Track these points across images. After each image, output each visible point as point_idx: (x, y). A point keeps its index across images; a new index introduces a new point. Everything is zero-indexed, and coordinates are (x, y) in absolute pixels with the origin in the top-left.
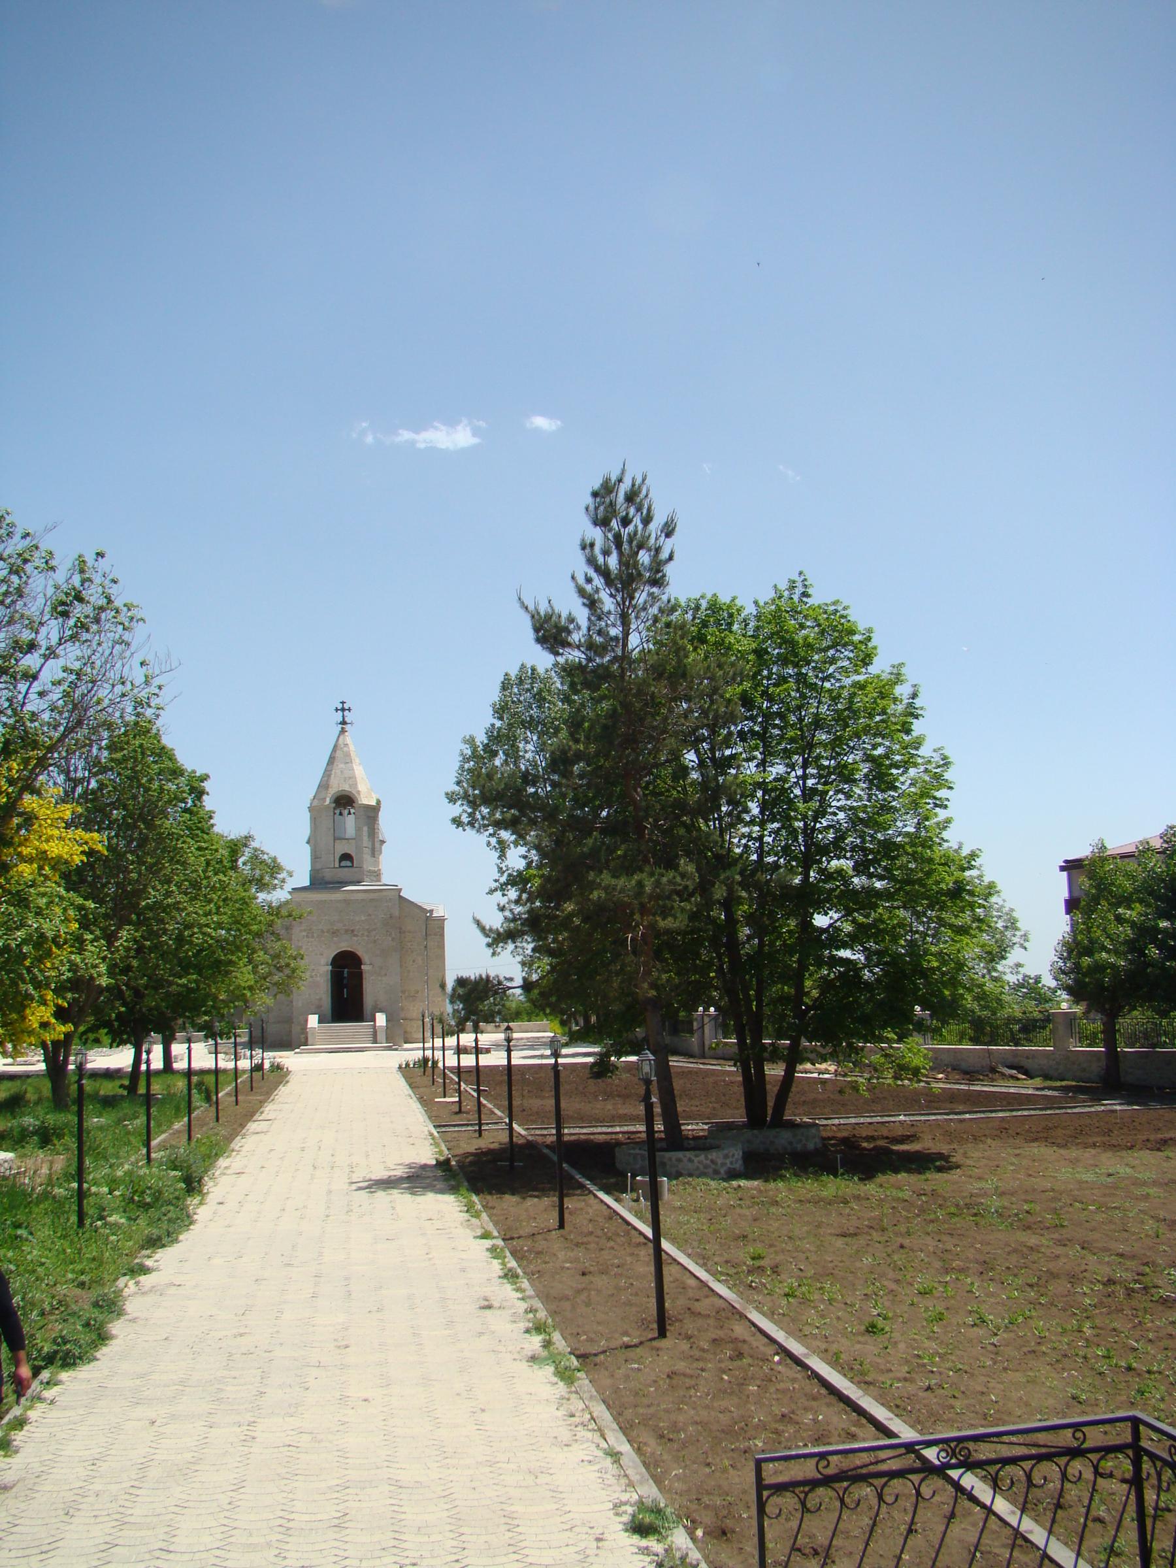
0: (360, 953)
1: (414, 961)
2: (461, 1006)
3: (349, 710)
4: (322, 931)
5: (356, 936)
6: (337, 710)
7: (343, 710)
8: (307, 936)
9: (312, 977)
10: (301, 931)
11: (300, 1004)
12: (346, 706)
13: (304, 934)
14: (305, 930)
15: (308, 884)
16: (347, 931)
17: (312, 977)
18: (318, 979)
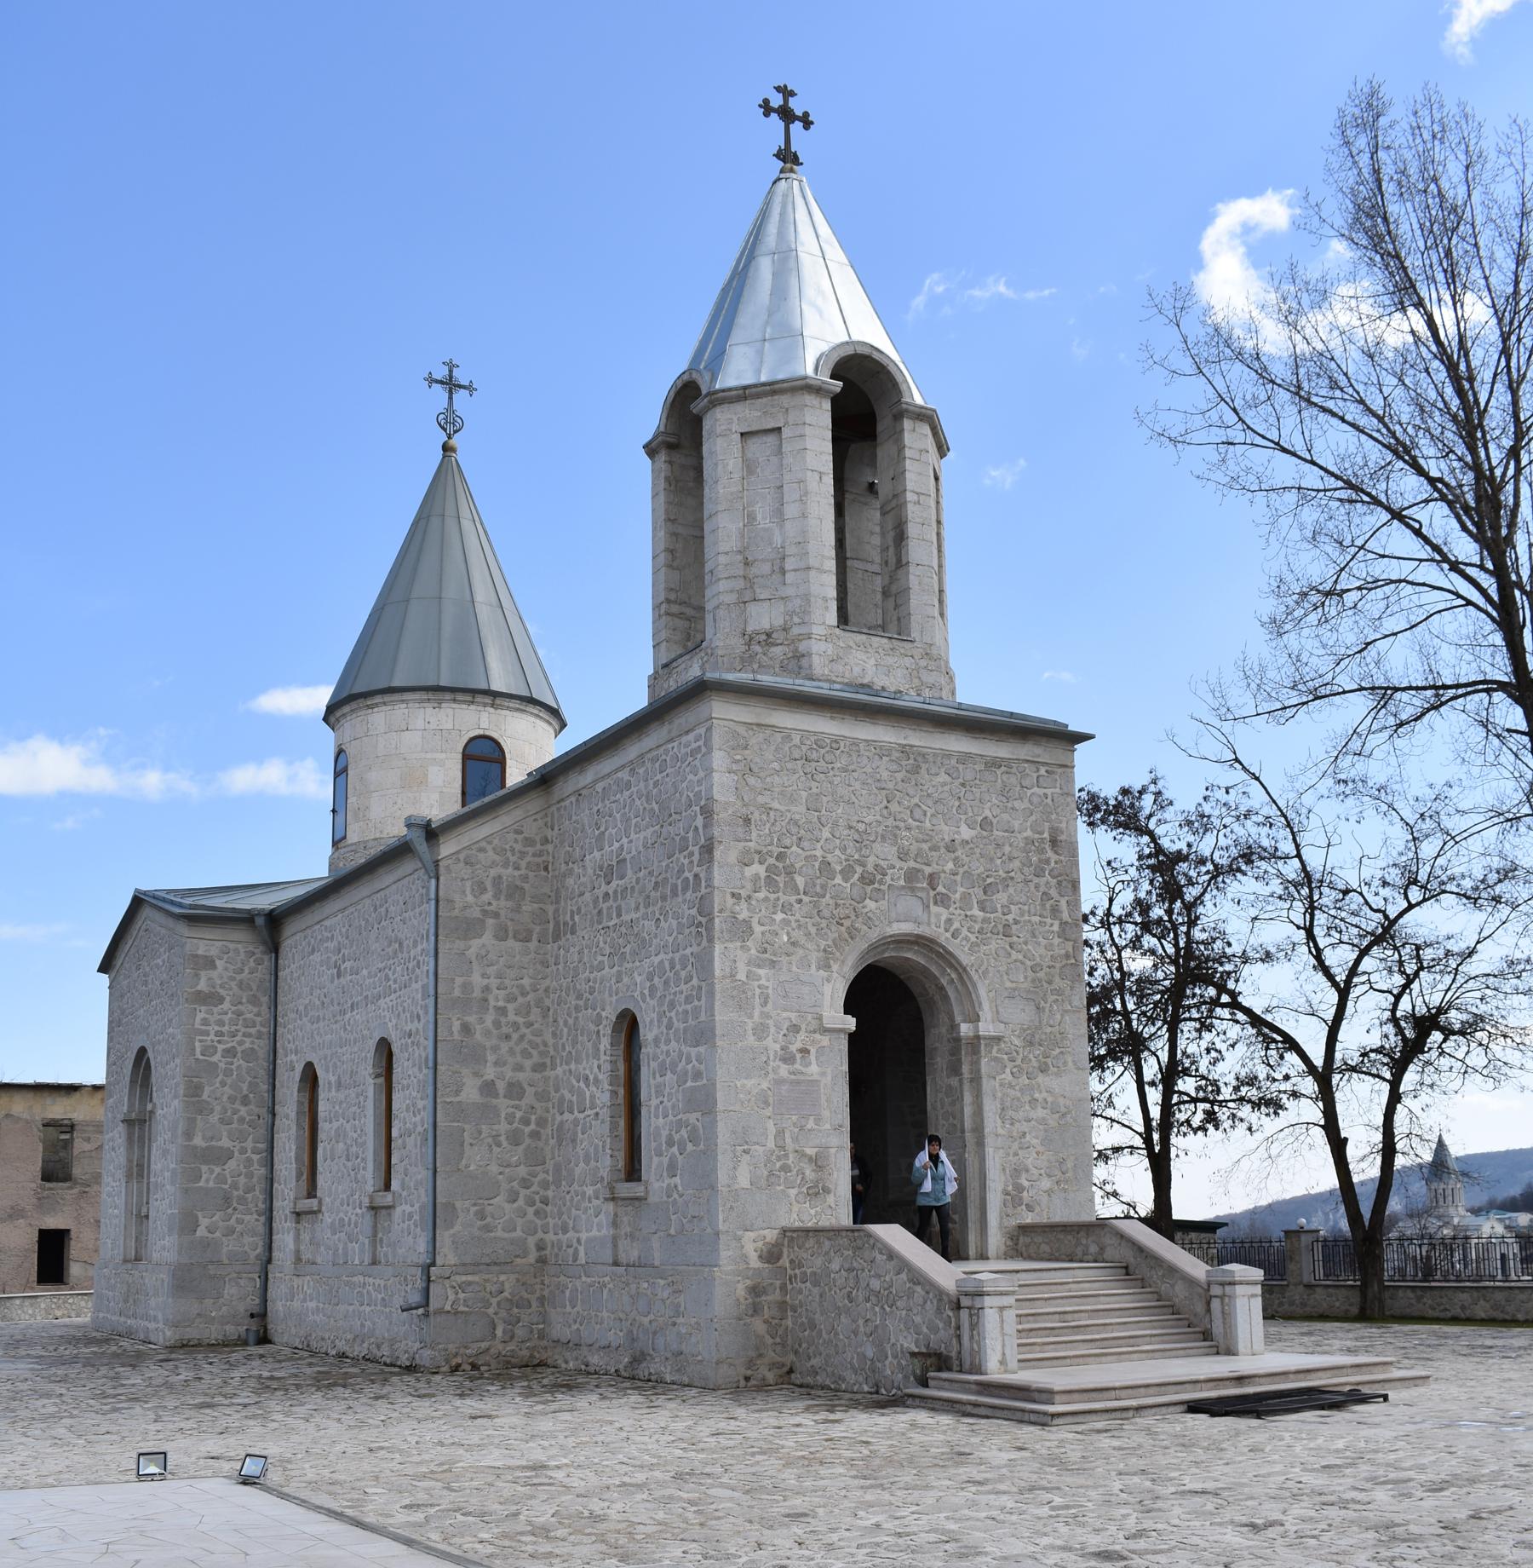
5: (942, 900)
9: (788, 1059)
11: (743, 1181)
13: (758, 869)
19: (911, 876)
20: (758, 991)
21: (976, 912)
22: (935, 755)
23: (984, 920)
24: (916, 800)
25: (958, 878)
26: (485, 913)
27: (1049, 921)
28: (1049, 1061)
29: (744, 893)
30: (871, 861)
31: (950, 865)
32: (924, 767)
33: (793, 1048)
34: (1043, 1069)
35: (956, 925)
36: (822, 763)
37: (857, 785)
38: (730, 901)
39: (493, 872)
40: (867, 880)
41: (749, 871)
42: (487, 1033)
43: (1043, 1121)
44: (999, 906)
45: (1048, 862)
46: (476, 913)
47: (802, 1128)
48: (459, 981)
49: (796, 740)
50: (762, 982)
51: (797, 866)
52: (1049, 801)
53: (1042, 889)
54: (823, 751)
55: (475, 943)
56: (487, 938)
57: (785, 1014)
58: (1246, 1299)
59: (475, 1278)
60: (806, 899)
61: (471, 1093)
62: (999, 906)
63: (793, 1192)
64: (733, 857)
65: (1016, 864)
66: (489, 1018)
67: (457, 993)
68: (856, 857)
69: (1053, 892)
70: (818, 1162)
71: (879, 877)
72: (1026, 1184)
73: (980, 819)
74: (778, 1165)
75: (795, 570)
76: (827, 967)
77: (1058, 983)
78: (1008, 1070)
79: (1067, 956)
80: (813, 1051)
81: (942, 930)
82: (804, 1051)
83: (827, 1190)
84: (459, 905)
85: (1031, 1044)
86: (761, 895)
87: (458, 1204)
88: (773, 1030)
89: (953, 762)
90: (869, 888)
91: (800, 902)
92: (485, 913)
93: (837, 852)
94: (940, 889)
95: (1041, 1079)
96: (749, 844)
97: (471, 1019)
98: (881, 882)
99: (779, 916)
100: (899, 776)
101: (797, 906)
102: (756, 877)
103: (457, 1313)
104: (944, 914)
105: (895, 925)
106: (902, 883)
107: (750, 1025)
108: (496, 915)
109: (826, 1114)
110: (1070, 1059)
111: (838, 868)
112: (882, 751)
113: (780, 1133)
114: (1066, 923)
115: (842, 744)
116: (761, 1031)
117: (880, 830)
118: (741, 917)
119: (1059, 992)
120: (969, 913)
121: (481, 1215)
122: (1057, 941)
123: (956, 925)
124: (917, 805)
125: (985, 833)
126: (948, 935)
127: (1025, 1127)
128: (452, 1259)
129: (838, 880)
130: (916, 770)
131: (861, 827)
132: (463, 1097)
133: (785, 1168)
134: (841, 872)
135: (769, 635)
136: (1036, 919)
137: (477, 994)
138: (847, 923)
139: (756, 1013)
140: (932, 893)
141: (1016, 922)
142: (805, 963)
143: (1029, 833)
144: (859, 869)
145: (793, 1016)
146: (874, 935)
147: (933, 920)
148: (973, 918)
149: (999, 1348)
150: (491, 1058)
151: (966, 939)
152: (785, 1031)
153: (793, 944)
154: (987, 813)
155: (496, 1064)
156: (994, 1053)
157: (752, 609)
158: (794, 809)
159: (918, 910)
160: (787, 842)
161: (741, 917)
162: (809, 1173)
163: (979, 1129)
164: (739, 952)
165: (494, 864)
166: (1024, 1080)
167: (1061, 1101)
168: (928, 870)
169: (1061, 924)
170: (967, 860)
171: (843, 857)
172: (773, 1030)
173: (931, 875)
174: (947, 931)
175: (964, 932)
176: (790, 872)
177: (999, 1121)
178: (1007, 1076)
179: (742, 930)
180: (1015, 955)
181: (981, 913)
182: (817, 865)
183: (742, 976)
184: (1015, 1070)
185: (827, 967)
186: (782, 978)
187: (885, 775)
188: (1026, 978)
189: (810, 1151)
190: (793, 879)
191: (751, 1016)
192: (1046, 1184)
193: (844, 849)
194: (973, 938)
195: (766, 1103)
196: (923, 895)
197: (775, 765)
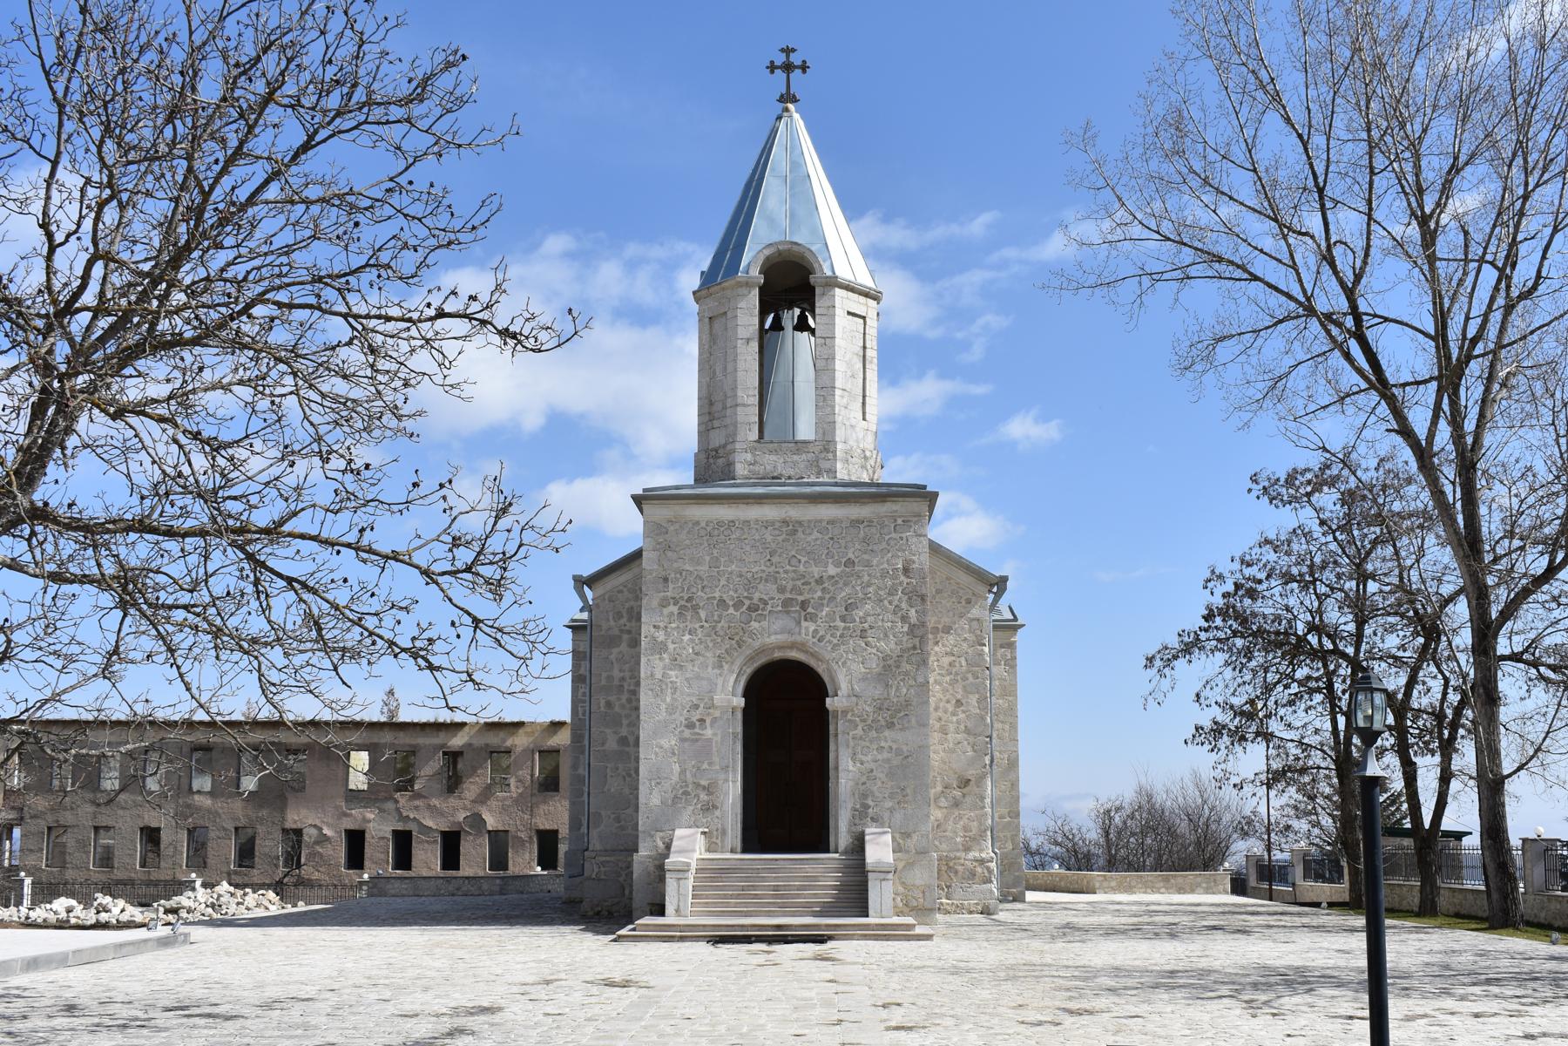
1: (959, 703)
2: (1392, 740)
3: (804, 67)
4: (722, 602)
5: (811, 618)
6: (772, 67)
7: (788, 68)
9: (691, 726)
11: (655, 800)
12: (796, 59)
13: (674, 609)
15: (688, 477)
17: (691, 726)
18: (709, 732)
19: (787, 603)
22: (809, 521)
23: (845, 628)
25: (825, 602)
26: (621, 631)
28: (895, 720)
29: (662, 624)
30: (757, 596)
31: (819, 594)
32: (800, 529)
34: (890, 725)
36: (722, 537)
37: (748, 548)
38: (652, 630)
39: (627, 605)
41: (666, 611)
42: (623, 706)
43: (888, 761)
45: (901, 583)
46: (616, 632)
47: (699, 769)
48: (604, 675)
49: (703, 524)
50: (674, 679)
53: (896, 603)
55: (615, 651)
56: (624, 647)
59: (612, 859)
60: (706, 625)
61: (612, 744)
64: (655, 603)
66: (624, 698)
67: (603, 682)
69: (904, 605)
72: (871, 803)
73: (844, 560)
76: (721, 667)
77: (906, 667)
78: (860, 728)
79: (914, 648)
82: (702, 721)
83: (715, 807)
84: (604, 626)
85: (880, 709)
86: (673, 625)
87: (603, 813)
89: (824, 524)
90: (754, 615)
91: (702, 627)
92: (621, 631)
93: (731, 593)
94: (810, 610)
95: (887, 733)
97: (612, 698)
98: (763, 609)
99: (687, 637)
100: (780, 538)
101: (700, 630)
102: (672, 613)
103: (599, 880)
104: (812, 627)
105: (773, 637)
107: (663, 706)
108: (629, 632)
109: (716, 759)
110: (913, 720)
111: (731, 603)
112: (767, 524)
113: (683, 772)
117: (764, 575)
118: (659, 640)
119: (907, 673)
121: (618, 820)
127: (872, 765)
128: (598, 847)
129: (731, 610)
131: (749, 575)
132: (607, 747)
133: (686, 793)
134: (734, 605)
137: (616, 682)
138: (737, 638)
139: (668, 700)
140: (803, 614)
141: (871, 627)
142: (704, 666)
144: (747, 602)
146: (757, 644)
147: (803, 631)
148: (836, 628)
150: (625, 722)
151: (830, 642)
153: (696, 654)
154: (851, 555)
155: (629, 725)
156: (849, 717)
157: (712, 432)
158: (699, 568)
159: (792, 624)
160: (694, 590)
161: (659, 640)
162: (703, 796)
163: (837, 768)
164: (657, 662)
165: (628, 600)
166: (873, 734)
167: (905, 748)
168: (800, 598)
170: (832, 589)
175: (828, 637)
176: (695, 608)
177: (851, 763)
178: (859, 731)
179: (660, 648)
183: (658, 676)
186: (688, 676)
187: (769, 538)
189: (704, 783)
191: (664, 701)
192: (888, 804)
193: (736, 591)
195: (674, 754)
196: (796, 615)
197: (687, 542)
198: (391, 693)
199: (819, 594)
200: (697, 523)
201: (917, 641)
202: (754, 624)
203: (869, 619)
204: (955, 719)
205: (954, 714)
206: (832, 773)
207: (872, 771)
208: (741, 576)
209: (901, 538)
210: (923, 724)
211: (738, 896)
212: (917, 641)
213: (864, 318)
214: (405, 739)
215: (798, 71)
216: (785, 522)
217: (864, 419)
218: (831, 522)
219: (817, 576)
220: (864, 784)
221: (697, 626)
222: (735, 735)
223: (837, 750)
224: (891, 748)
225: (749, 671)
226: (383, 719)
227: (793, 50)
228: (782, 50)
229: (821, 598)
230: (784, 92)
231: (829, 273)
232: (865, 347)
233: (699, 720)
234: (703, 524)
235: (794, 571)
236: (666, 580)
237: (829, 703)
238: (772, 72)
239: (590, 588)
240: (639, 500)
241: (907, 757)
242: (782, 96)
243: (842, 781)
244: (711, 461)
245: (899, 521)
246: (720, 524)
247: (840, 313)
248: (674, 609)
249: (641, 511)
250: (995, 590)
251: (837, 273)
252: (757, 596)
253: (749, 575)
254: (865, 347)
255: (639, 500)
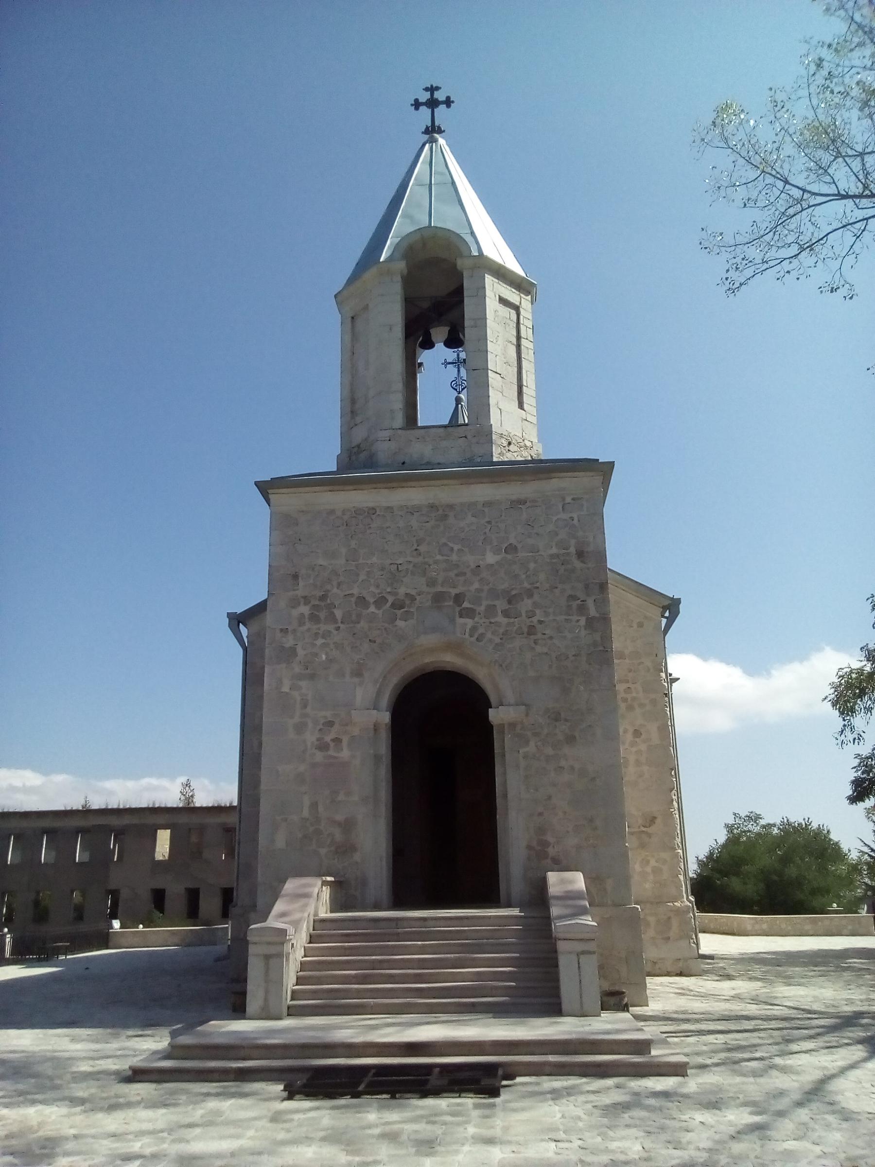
0: (481, 675)
1: (637, 733)
3: (448, 102)
4: (362, 601)
5: (469, 613)
6: (417, 105)
7: (433, 104)
8: (314, 618)
9: (323, 747)
10: (294, 603)
11: (280, 842)
12: (440, 96)
13: (305, 610)
14: (306, 600)
16: (438, 598)
17: (323, 747)
18: (345, 754)
19: (438, 598)
20: (298, 698)
21: (500, 619)
23: (509, 624)
24: (443, 540)
27: (575, 618)
29: (290, 628)
33: (328, 739)
34: (571, 740)
35: (481, 630)
38: (279, 635)
40: (398, 605)
41: (295, 613)
44: (524, 614)
49: (339, 513)
51: (337, 603)
52: (576, 521)
54: (361, 517)
57: (323, 713)
58: (574, 958)
60: (342, 626)
62: (524, 614)
63: (323, 851)
65: (542, 576)
68: (389, 590)
69: (581, 595)
70: (348, 826)
71: (407, 602)
74: (311, 829)
75: (373, 397)
76: (358, 673)
78: (532, 744)
80: (345, 740)
81: (467, 634)
82: (337, 741)
85: (556, 720)
86: (305, 628)
88: (310, 725)
90: (399, 612)
91: (338, 629)
93: (372, 589)
94: (466, 605)
96: (297, 592)
101: (335, 632)
104: (469, 622)
106: (429, 603)
111: (372, 600)
112: (412, 511)
113: (314, 806)
114: (593, 618)
115: (378, 510)
116: (300, 728)
120: (493, 621)
122: (583, 633)
123: (481, 630)
124: (445, 544)
125: (509, 557)
126: (473, 639)
129: (372, 609)
130: (445, 517)
135: (358, 446)
136: (563, 617)
140: (458, 609)
143: (554, 550)
144: (391, 599)
145: (328, 714)
148: (498, 624)
149: (261, 994)
152: (321, 727)
154: (512, 541)
160: (328, 587)
161: (287, 645)
163: (505, 796)
166: (549, 751)
168: (454, 592)
169: (587, 619)
171: (377, 591)
172: (310, 725)
173: (456, 595)
174: (471, 636)
175: (489, 635)
178: (531, 748)
180: (539, 649)
181: (504, 620)
182: (353, 600)
183: (286, 689)
184: (539, 743)
185: (358, 673)
188: (550, 667)
189: (339, 817)
190: (333, 613)
193: (378, 586)
194: (497, 640)
198: (188, 785)
199: (476, 585)
200: (332, 512)
201: (597, 637)
202: (400, 623)
203: (538, 611)
204: (634, 749)
205: (633, 744)
206: (499, 801)
207: (550, 798)
208: (383, 569)
209: (572, 519)
210: (612, 737)
211: (364, 979)
212: (597, 637)
213: (517, 309)
214: (195, 820)
215: (443, 107)
216: (432, 507)
217: (521, 406)
218: (488, 504)
219: (473, 566)
220: (540, 814)
221: (331, 627)
222: (377, 758)
223: (505, 773)
224: (572, 768)
225: (394, 680)
226: (181, 805)
227: (437, 88)
228: (426, 89)
229: (478, 591)
230: (429, 125)
231: (476, 253)
232: (519, 337)
233: (333, 740)
234: (339, 513)
235: (446, 561)
236: (295, 577)
237: (495, 716)
238: (417, 108)
239: (245, 625)
240: (265, 488)
241: (593, 779)
242: (427, 128)
243: (512, 814)
244: (354, 458)
245: (568, 500)
246: (358, 512)
247: (489, 293)
248: (305, 610)
249: (268, 501)
250: (667, 614)
251: (486, 253)
252: (402, 591)
253: (394, 567)
254: (519, 337)
255: (265, 488)
